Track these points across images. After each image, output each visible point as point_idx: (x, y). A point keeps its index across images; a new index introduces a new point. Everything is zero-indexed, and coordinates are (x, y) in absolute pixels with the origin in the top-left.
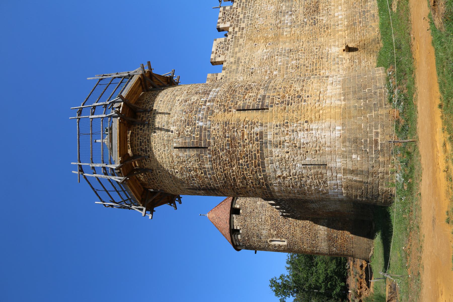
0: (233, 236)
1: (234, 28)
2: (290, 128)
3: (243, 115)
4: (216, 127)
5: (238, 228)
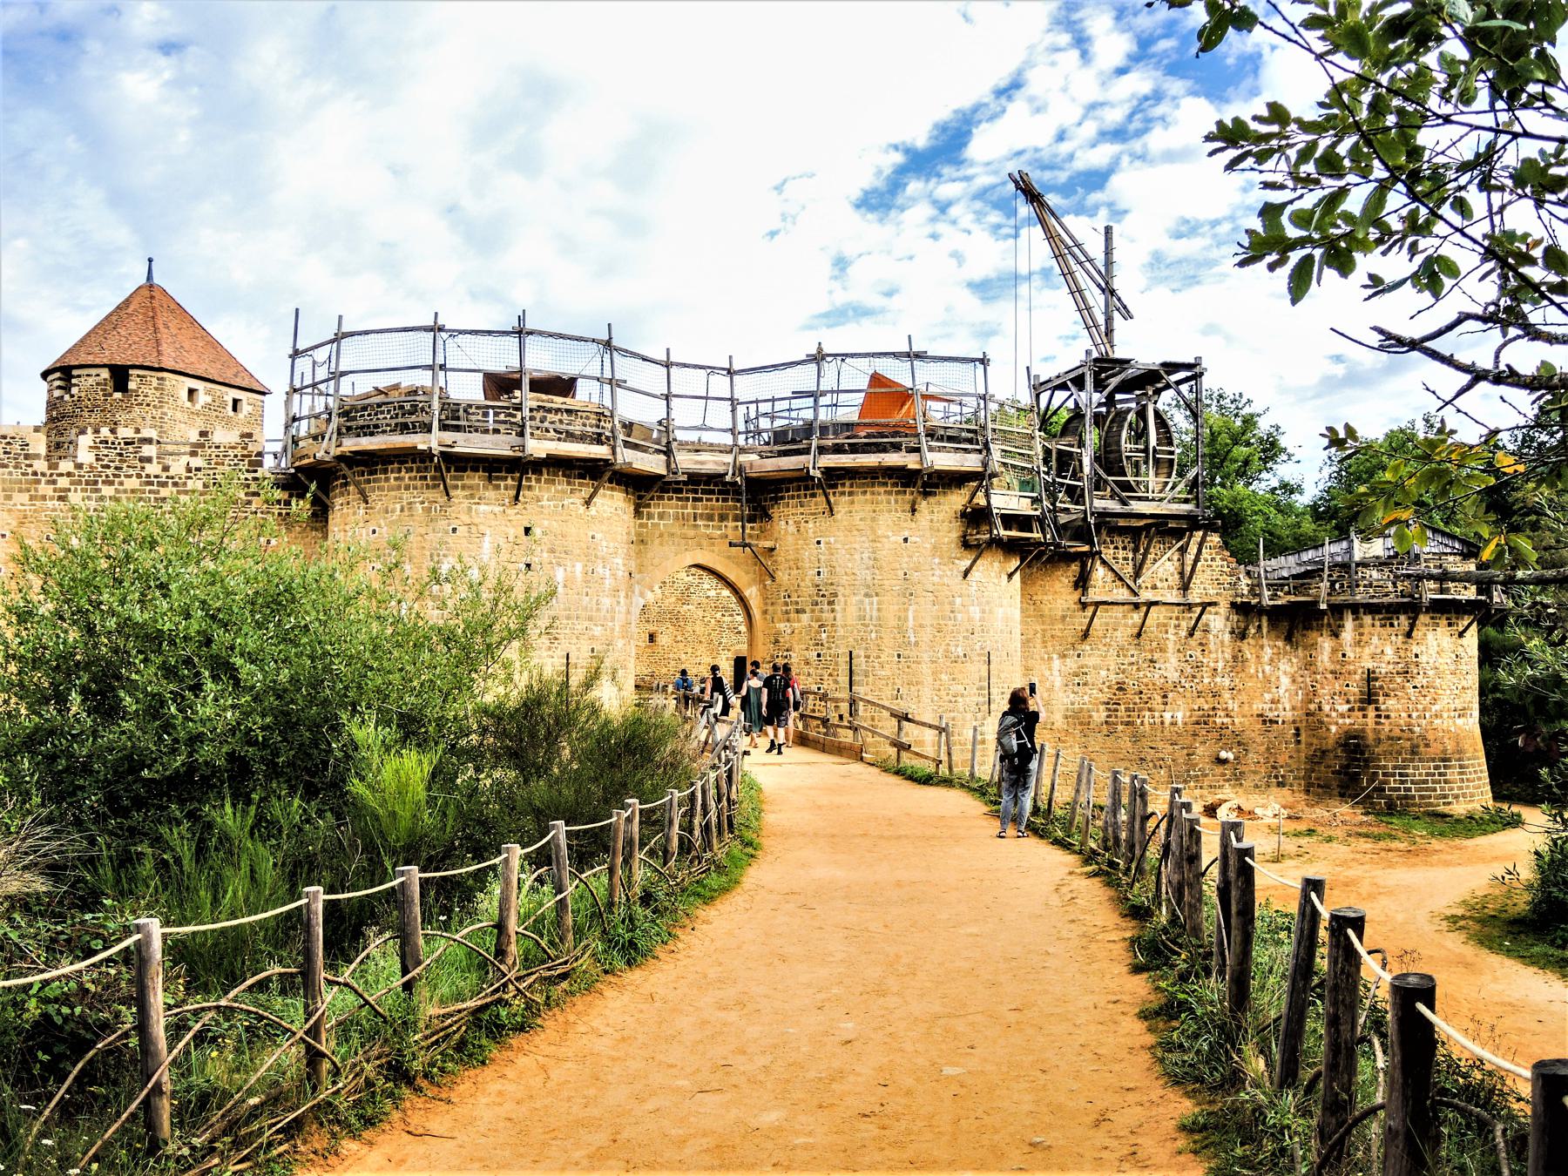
0: (58, 375)
1: (69, 474)
5: (74, 390)
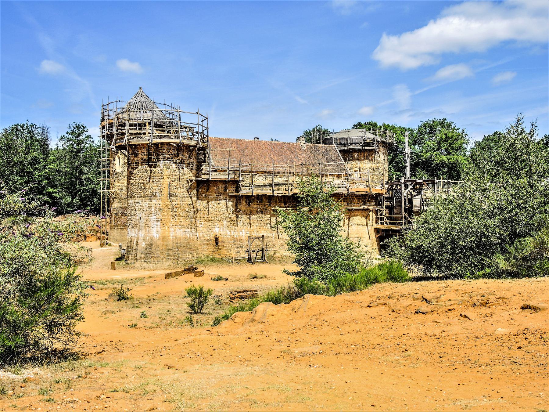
2: (158, 212)
3: (166, 186)
4: (160, 172)
